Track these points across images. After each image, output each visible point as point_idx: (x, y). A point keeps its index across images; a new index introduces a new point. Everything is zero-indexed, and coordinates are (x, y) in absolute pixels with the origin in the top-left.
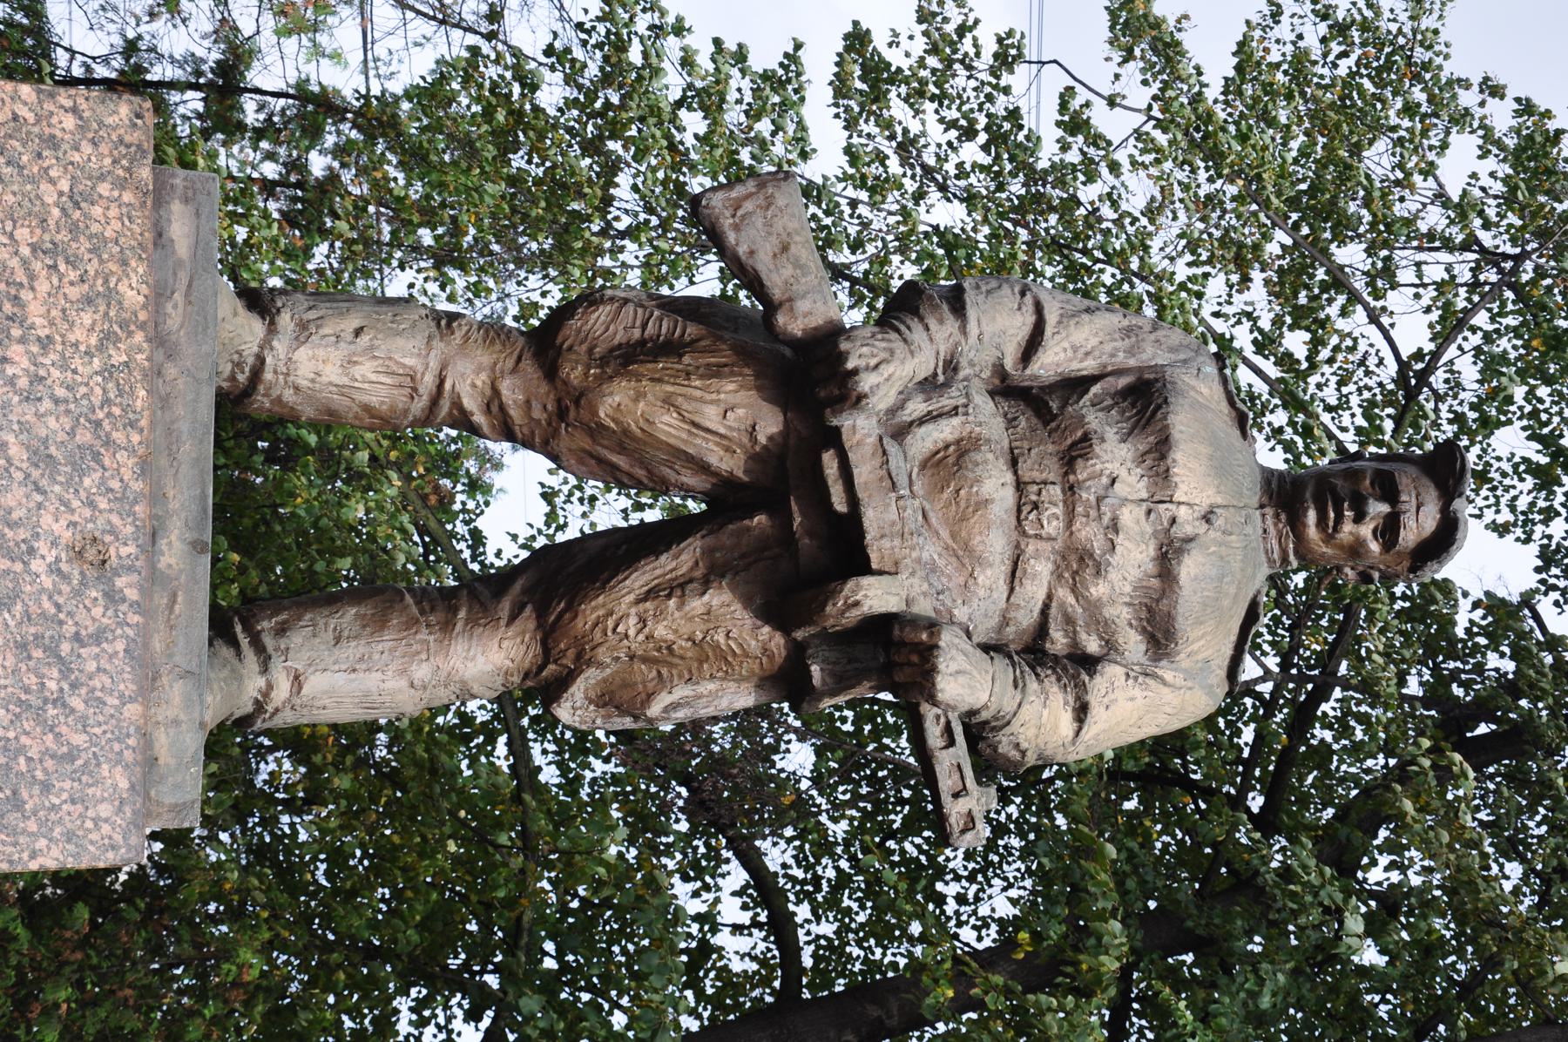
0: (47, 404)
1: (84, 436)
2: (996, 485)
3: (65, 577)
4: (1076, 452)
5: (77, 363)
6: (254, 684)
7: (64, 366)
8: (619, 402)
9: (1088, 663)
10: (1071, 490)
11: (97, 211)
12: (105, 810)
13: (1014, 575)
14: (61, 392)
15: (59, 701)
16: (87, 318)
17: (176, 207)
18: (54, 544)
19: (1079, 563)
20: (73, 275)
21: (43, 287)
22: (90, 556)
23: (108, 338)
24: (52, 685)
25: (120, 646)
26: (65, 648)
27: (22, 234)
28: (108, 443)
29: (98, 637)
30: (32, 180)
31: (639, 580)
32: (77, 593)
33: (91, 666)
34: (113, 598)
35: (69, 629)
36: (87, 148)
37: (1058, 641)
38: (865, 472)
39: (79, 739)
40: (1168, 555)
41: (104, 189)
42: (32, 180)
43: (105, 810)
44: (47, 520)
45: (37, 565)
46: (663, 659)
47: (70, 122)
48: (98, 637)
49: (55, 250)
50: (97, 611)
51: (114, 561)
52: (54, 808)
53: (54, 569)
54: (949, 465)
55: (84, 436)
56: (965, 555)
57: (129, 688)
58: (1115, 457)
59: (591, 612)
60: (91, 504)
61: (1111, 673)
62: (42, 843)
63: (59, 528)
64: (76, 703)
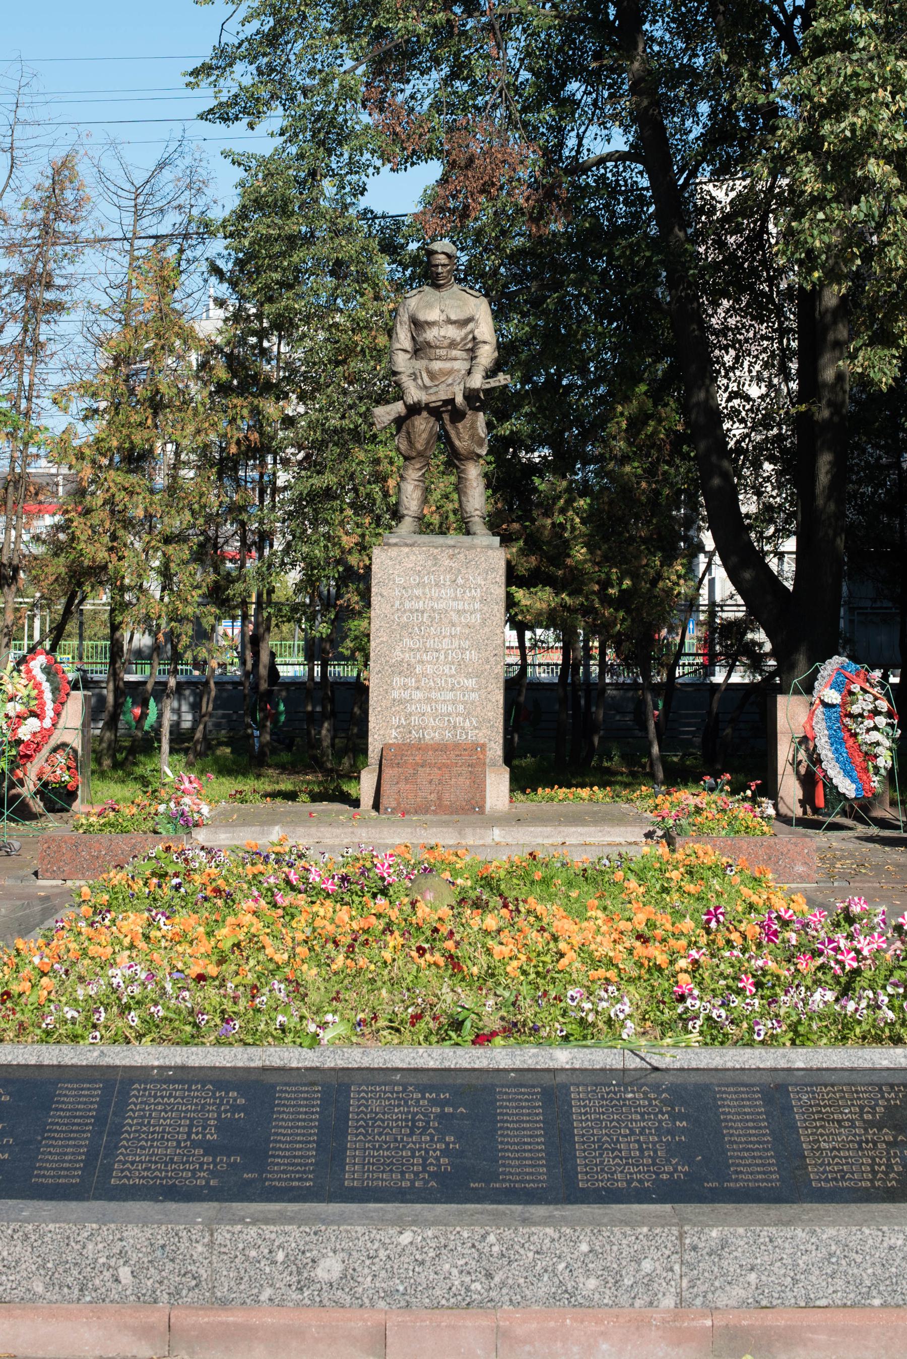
2: (436, 365)
4: (428, 344)
6: (477, 519)
8: (420, 446)
9: (474, 338)
10: (437, 347)
13: (456, 359)
19: (453, 345)
22: (451, 557)
31: (457, 443)
37: (470, 345)
38: (434, 398)
40: (449, 322)
46: (472, 437)
54: (432, 375)
56: (450, 372)
58: (431, 335)
59: (462, 451)
61: (477, 333)
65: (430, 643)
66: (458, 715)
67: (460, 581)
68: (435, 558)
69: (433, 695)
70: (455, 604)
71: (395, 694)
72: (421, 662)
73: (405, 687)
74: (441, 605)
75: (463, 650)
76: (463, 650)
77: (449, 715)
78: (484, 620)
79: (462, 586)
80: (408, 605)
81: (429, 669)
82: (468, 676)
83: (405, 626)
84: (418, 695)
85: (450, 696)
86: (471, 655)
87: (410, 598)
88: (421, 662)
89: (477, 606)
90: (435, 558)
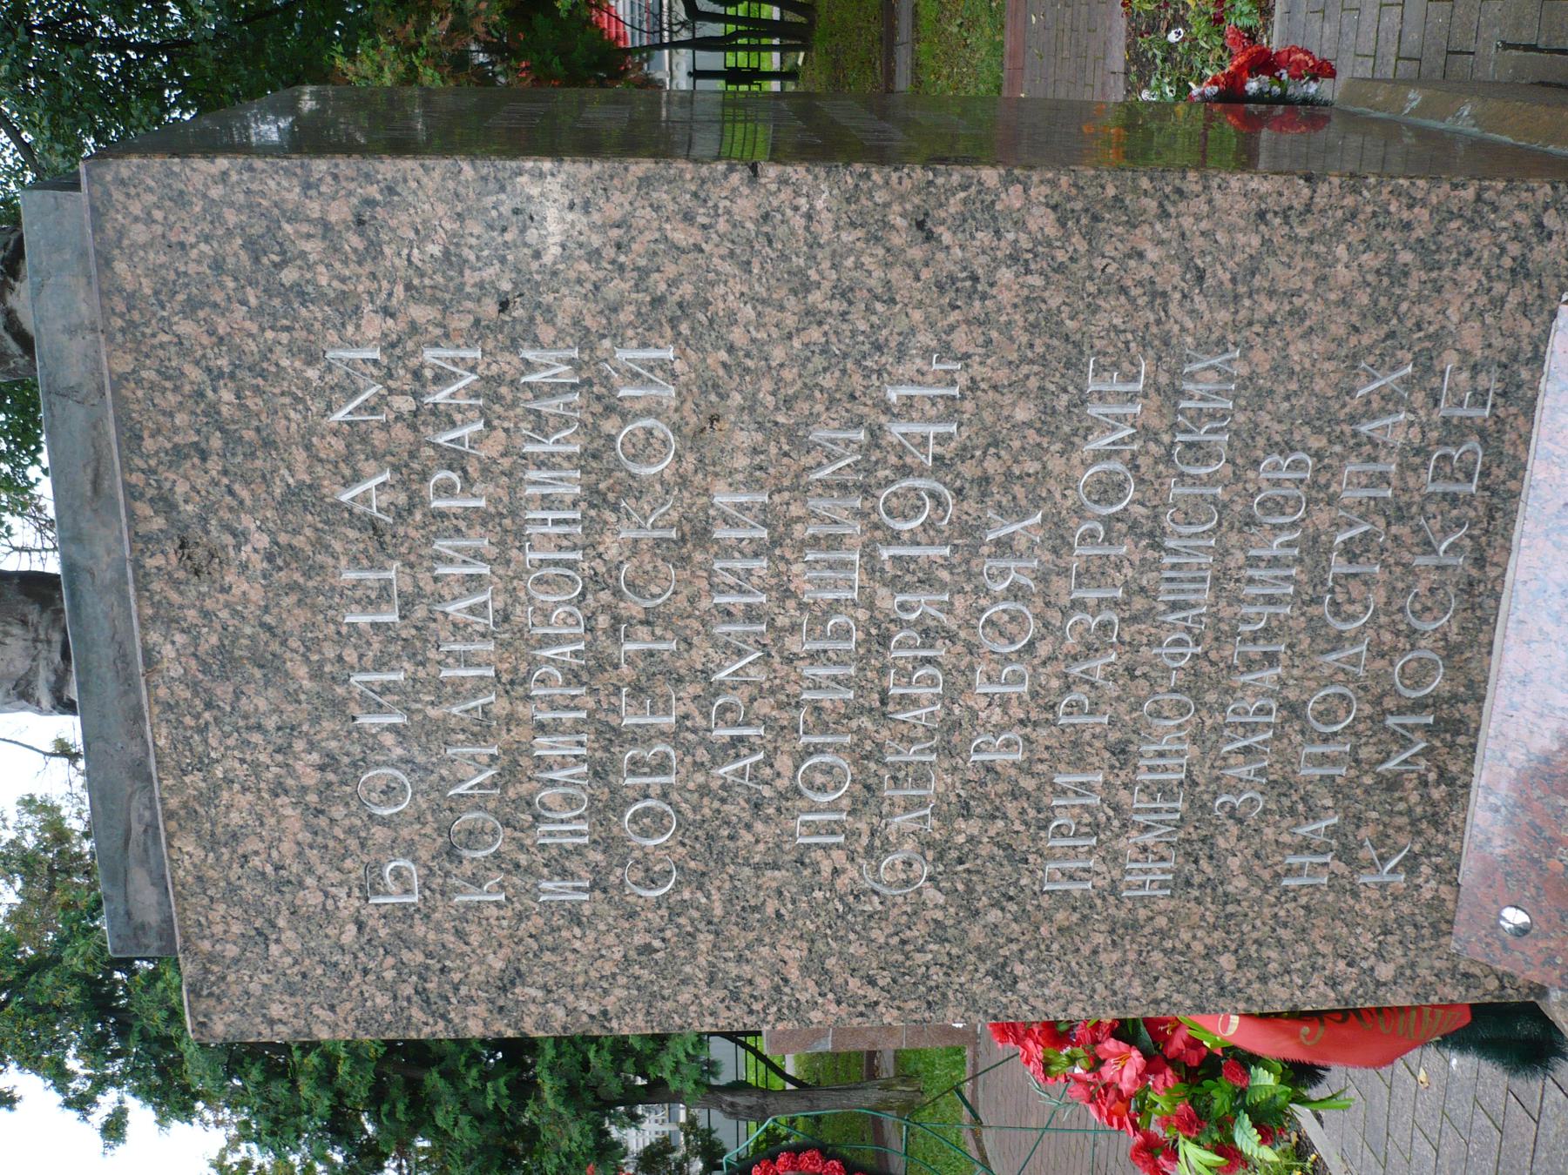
0: (271, 723)
1: (223, 692)
3: (228, 528)
5: (242, 771)
7: (256, 766)
11: (236, 928)
12: (139, 233)
14: (256, 738)
15: (216, 376)
16: (235, 818)
17: (153, 918)
18: (244, 567)
20: (256, 861)
21: (287, 847)
23: (209, 797)
24: (227, 396)
25: (149, 444)
26: (216, 442)
27: (315, 899)
28: (194, 686)
29: (178, 454)
30: (311, 952)
32: (209, 509)
33: (181, 419)
34: (164, 503)
35: (215, 466)
36: (255, 988)
39: (185, 327)
41: (232, 951)
42: (311, 952)
43: (139, 233)
44: (256, 594)
45: (262, 541)
47: (276, 1011)
48: (178, 454)
49: (279, 886)
50: (181, 488)
51: (171, 548)
52: (207, 239)
53: (241, 537)
55: (223, 692)
57: (132, 392)
60: (206, 614)
62: (216, 192)
63: (241, 586)
64: (194, 373)
65: (825, 684)
66: (1320, 492)
67: (371, 490)
68: (224, 661)
69: (1173, 655)
70: (542, 524)
71: (1147, 878)
72: (950, 736)
73: (1103, 826)
74: (560, 622)
75: (878, 463)
76: (878, 463)
77: (1314, 546)
78: (659, 315)
79: (410, 474)
80: (566, 828)
81: (999, 684)
82: (1063, 425)
83: (710, 845)
84: (1168, 747)
85: (1189, 544)
86: (919, 406)
87: (521, 814)
88: (950, 736)
89: (550, 364)
90: (224, 661)
